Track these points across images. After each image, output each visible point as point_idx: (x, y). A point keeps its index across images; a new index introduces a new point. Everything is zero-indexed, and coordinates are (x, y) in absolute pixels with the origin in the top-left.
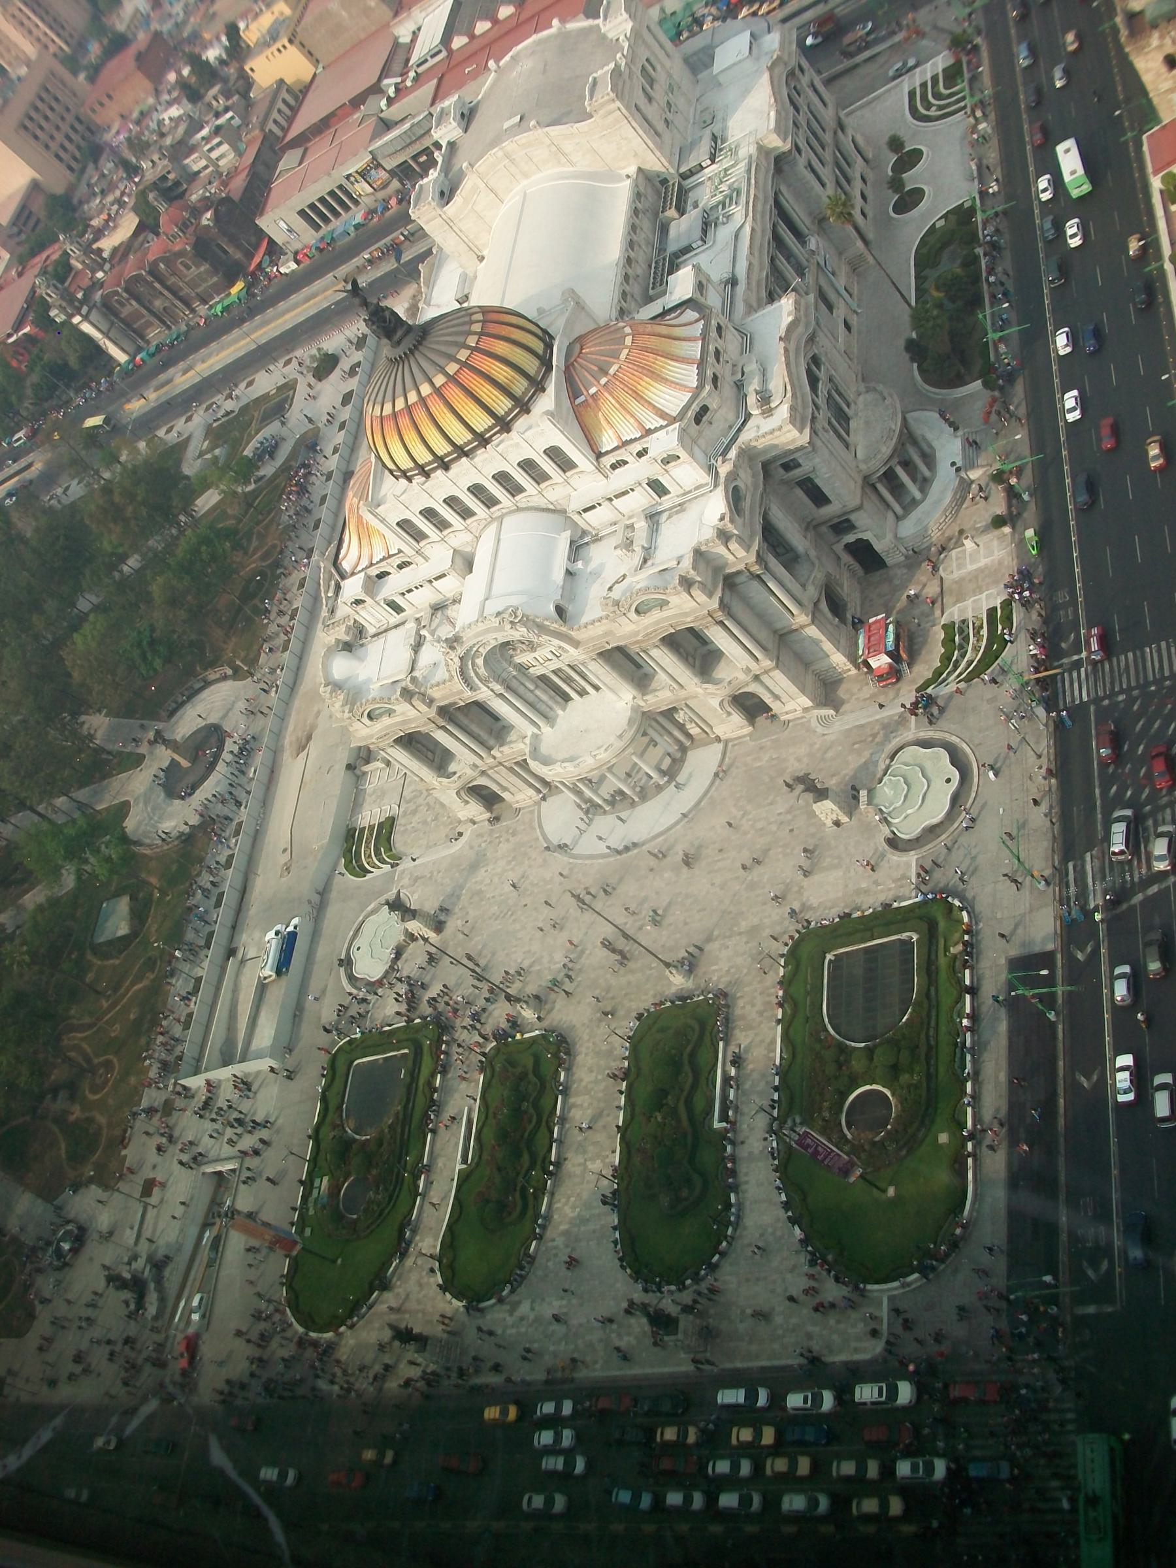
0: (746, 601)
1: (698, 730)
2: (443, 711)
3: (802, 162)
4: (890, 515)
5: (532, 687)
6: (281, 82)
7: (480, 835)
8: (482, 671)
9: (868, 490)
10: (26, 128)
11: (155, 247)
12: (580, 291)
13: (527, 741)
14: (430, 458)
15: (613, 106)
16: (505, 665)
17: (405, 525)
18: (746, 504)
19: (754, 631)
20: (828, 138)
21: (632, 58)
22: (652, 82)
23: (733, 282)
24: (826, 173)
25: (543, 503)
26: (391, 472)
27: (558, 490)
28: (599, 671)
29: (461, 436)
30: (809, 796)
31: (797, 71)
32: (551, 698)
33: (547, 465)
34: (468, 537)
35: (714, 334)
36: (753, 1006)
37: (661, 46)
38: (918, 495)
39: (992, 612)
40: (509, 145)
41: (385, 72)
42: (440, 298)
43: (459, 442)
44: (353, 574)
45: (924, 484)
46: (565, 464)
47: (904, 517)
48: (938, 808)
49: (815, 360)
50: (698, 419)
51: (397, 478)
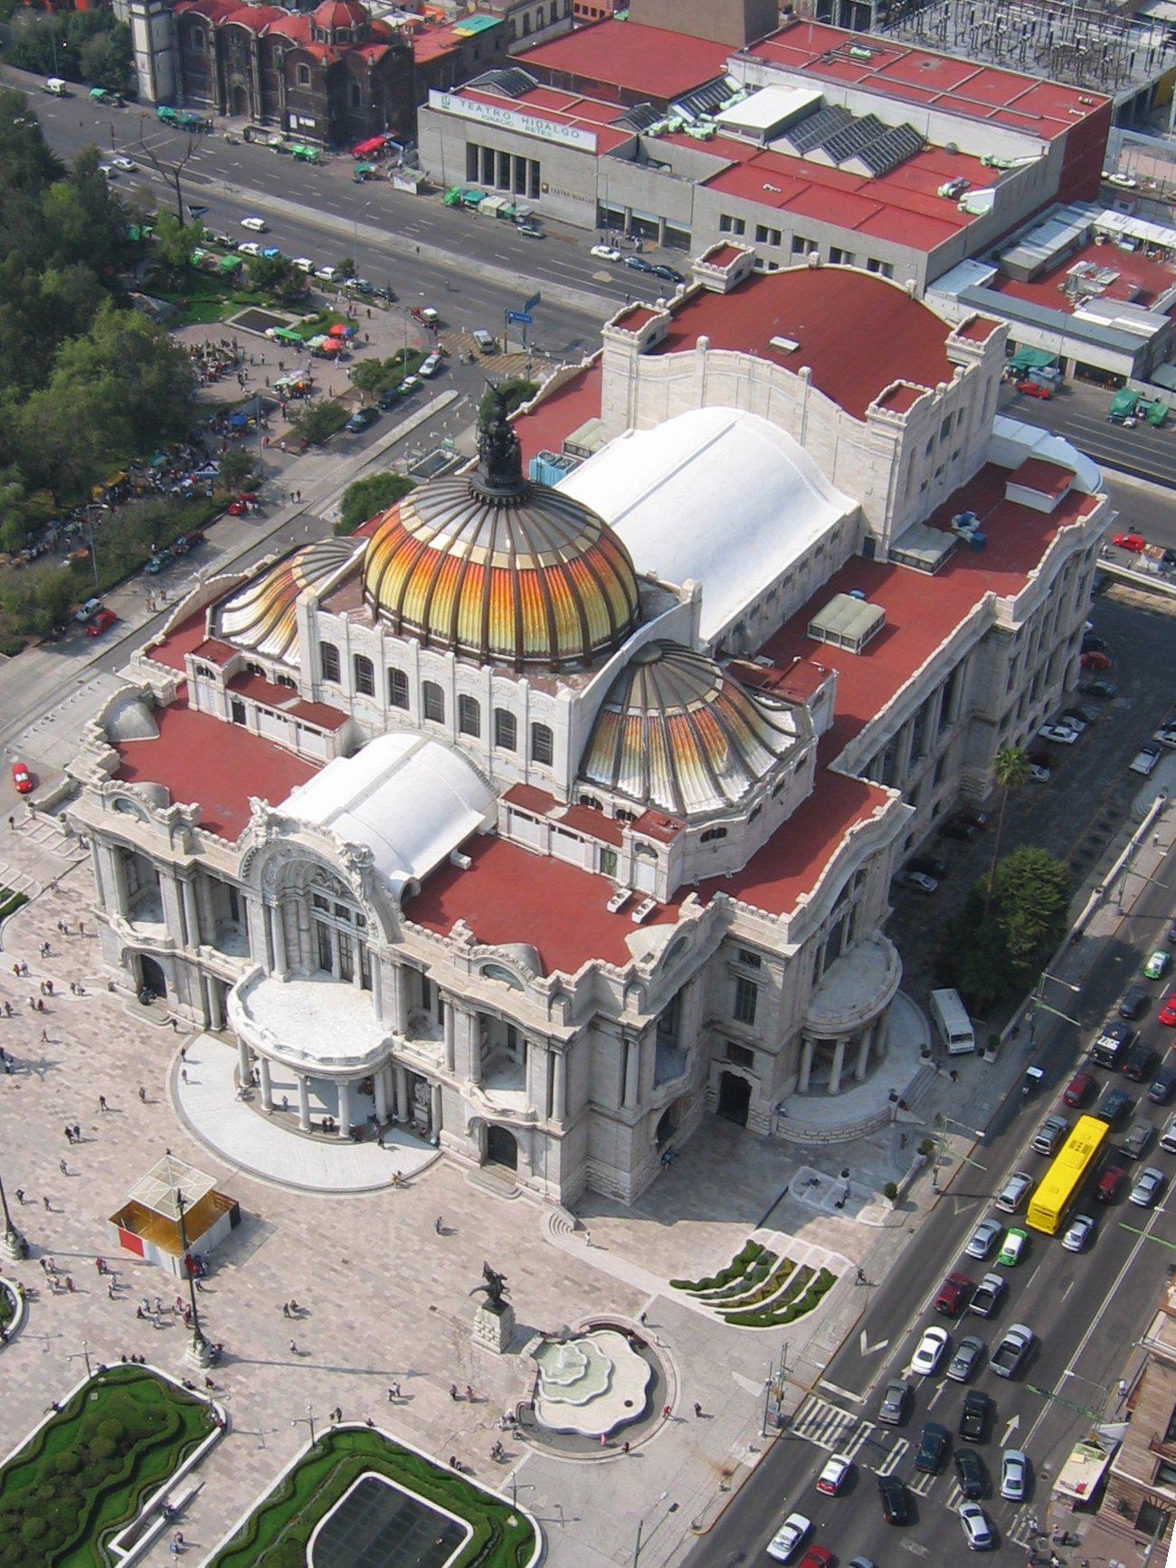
0: (592, 1050)
1: (425, 1117)
2: (196, 866)
3: (1011, 650)
4: (792, 1080)
7: (108, 1009)
8: (275, 871)
9: (795, 1044)
13: (249, 971)
14: (419, 618)
15: (894, 434)
16: (300, 884)
18: (678, 963)
19: (573, 1088)
20: (1052, 643)
21: (949, 397)
24: (1022, 679)
25: (483, 766)
27: (513, 766)
28: (387, 978)
29: (470, 630)
30: (483, 1297)
31: (1083, 556)
32: (312, 952)
33: (522, 737)
34: (379, 723)
35: (793, 765)
36: (251, 1455)
37: (985, 406)
38: (834, 1086)
39: (807, 1271)
40: (765, 367)
41: (682, 98)
42: (573, 486)
43: (464, 634)
45: (849, 1080)
47: (801, 1094)
48: (596, 1421)
49: (859, 876)
50: (706, 836)
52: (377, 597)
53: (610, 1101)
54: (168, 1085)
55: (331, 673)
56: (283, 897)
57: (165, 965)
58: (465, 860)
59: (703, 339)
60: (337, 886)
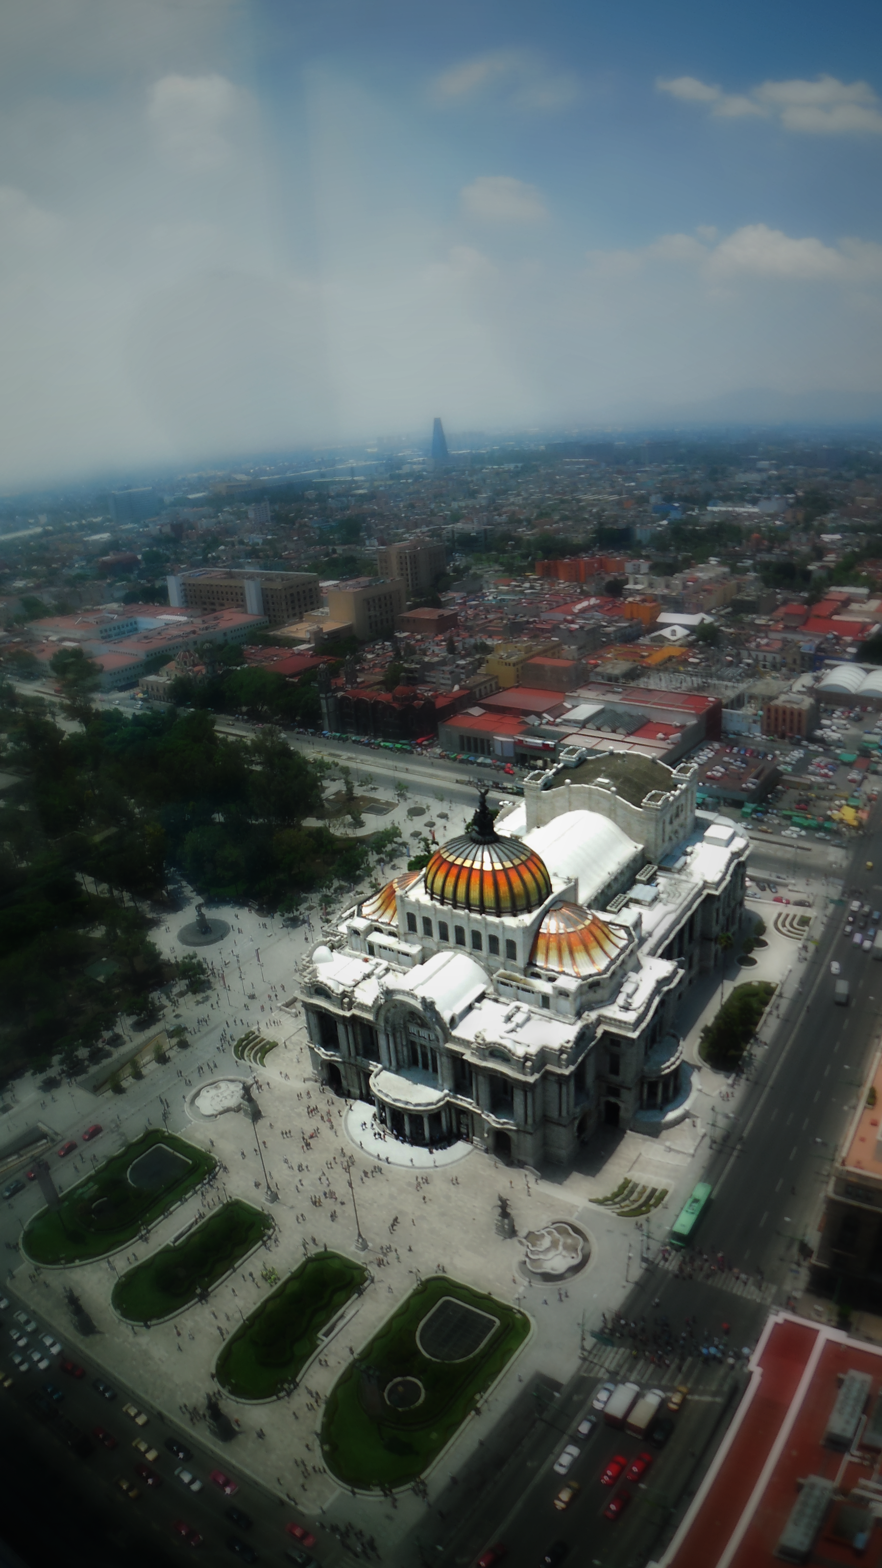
5: (404, 1043)
6: (497, 677)
10: (369, 603)
11: (384, 697)
12: (580, 882)
16: (402, 1022)
17: (411, 918)
21: (677, 798)
22: (677, 815)
23: (650, 934)
26: (426, 887)
28: (443, 1064)
33: (502, 946)
41: (548, 711)
43: (472, 902)
44: (364, 917)
46: (511, 954)
49: (662, 1003)
51: (426, 892)
52: (432, 890)
53: (554, 1114)
54: (343, 1123)
55: (412, 927)
56: (394, 1029)
57: (341, 1068)
58: (477, 1005)
59: (568, 781)
60: (419, 1021)
